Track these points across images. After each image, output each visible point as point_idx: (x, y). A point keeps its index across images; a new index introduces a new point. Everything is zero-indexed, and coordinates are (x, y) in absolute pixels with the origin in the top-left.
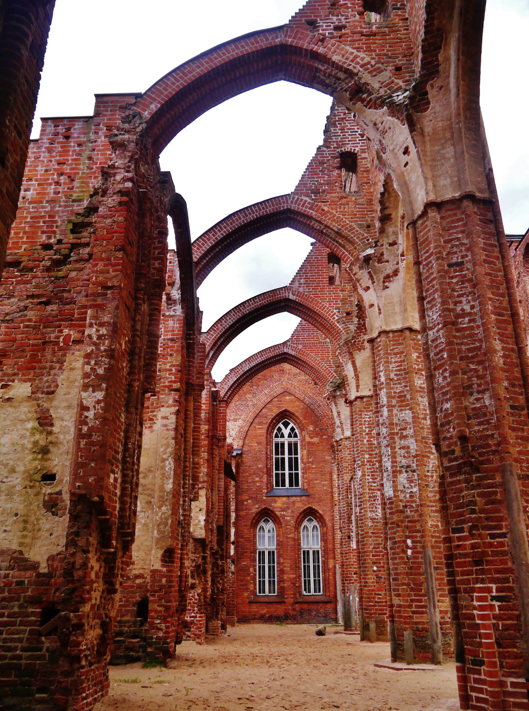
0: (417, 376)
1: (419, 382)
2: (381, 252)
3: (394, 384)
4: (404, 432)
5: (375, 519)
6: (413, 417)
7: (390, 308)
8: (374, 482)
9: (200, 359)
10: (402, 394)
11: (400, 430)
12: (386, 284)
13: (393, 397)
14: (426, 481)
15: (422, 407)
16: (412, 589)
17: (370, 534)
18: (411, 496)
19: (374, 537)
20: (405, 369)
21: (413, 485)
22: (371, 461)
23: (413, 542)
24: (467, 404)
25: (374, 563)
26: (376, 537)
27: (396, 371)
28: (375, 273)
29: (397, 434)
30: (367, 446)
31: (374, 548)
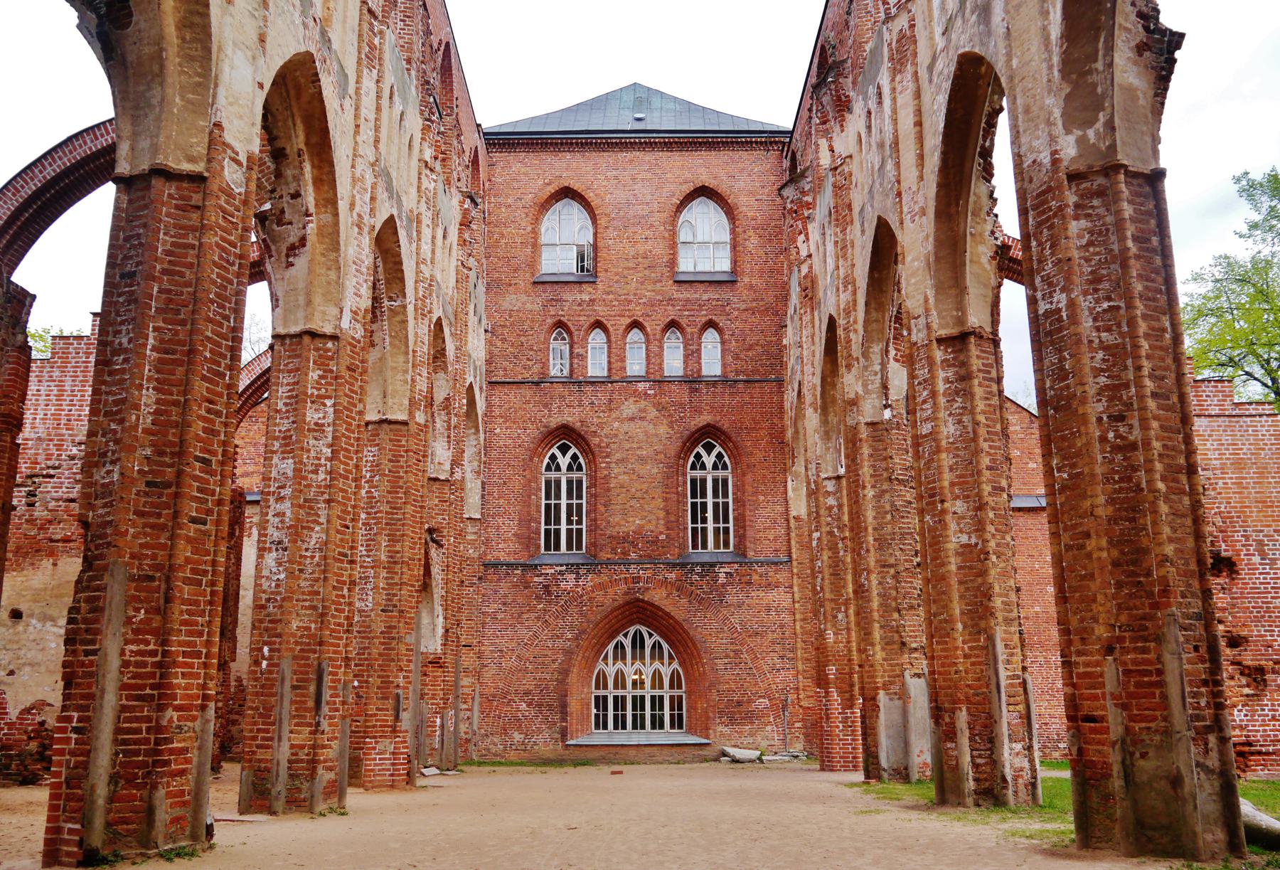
0: (315, 406)
1: (316, 416)
2: (280, 207)
3: (281, 418)
4: (282, 491)
5: (364, 611)
6: (295, 470)
7: (292, 298)
8: (368, 556)
9: (9, 375)
10: (288, 434)
11: (279, 487)
12: (291, 259)
13: (276, 439)
14: (300, 563)
15: (313, 454)
16: (261, 715)
17: (355, 634)
18: (277, 586)
19: (360, 637)
20: (297, 395)
21: (281, 569)
22: (368, 524)
23: (270, 650)
24: (98, 478)
25: (355, 676)
26: (363, 638)
27: (287, 397)
28: (274, 242)
29: (274, 493)
30: (365, 500)
31: (358, 654)
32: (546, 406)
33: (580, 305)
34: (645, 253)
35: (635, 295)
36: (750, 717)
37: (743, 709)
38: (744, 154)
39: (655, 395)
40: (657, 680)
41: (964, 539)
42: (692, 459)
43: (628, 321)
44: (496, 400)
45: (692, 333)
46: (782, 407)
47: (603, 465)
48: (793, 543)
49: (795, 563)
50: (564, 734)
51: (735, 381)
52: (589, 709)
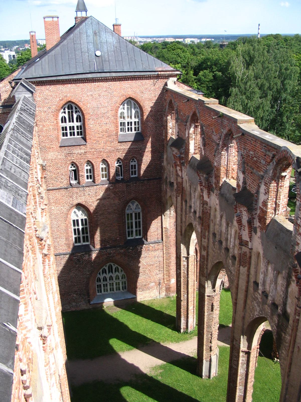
32: (71, 197)
33: (80, 155)
34: (106, 130)
35: (103, 148)
36: (149, 289)
37: (147, 286)
38: (147, 81)
39: (113, 189)
40: (117, 278)
41: (241, 394)
42: (127, 208)
43: (101, 159)
44: (51, 197)
45: (126, 163)
46: (161, 189)
47: (95, 216)
48: (164, 236)
49: (164, 242)
50: (89, 301)
51: (144, 180)
52: (95, 289)
